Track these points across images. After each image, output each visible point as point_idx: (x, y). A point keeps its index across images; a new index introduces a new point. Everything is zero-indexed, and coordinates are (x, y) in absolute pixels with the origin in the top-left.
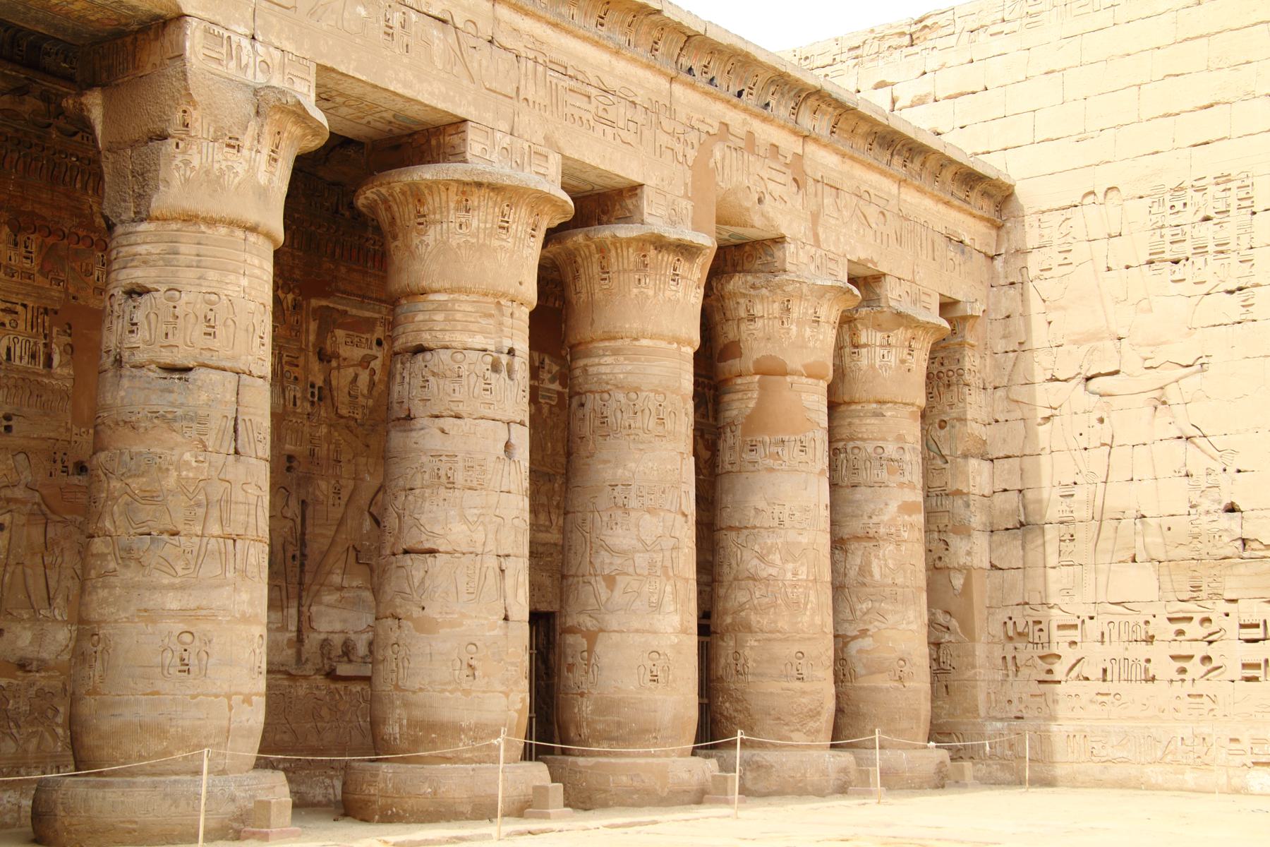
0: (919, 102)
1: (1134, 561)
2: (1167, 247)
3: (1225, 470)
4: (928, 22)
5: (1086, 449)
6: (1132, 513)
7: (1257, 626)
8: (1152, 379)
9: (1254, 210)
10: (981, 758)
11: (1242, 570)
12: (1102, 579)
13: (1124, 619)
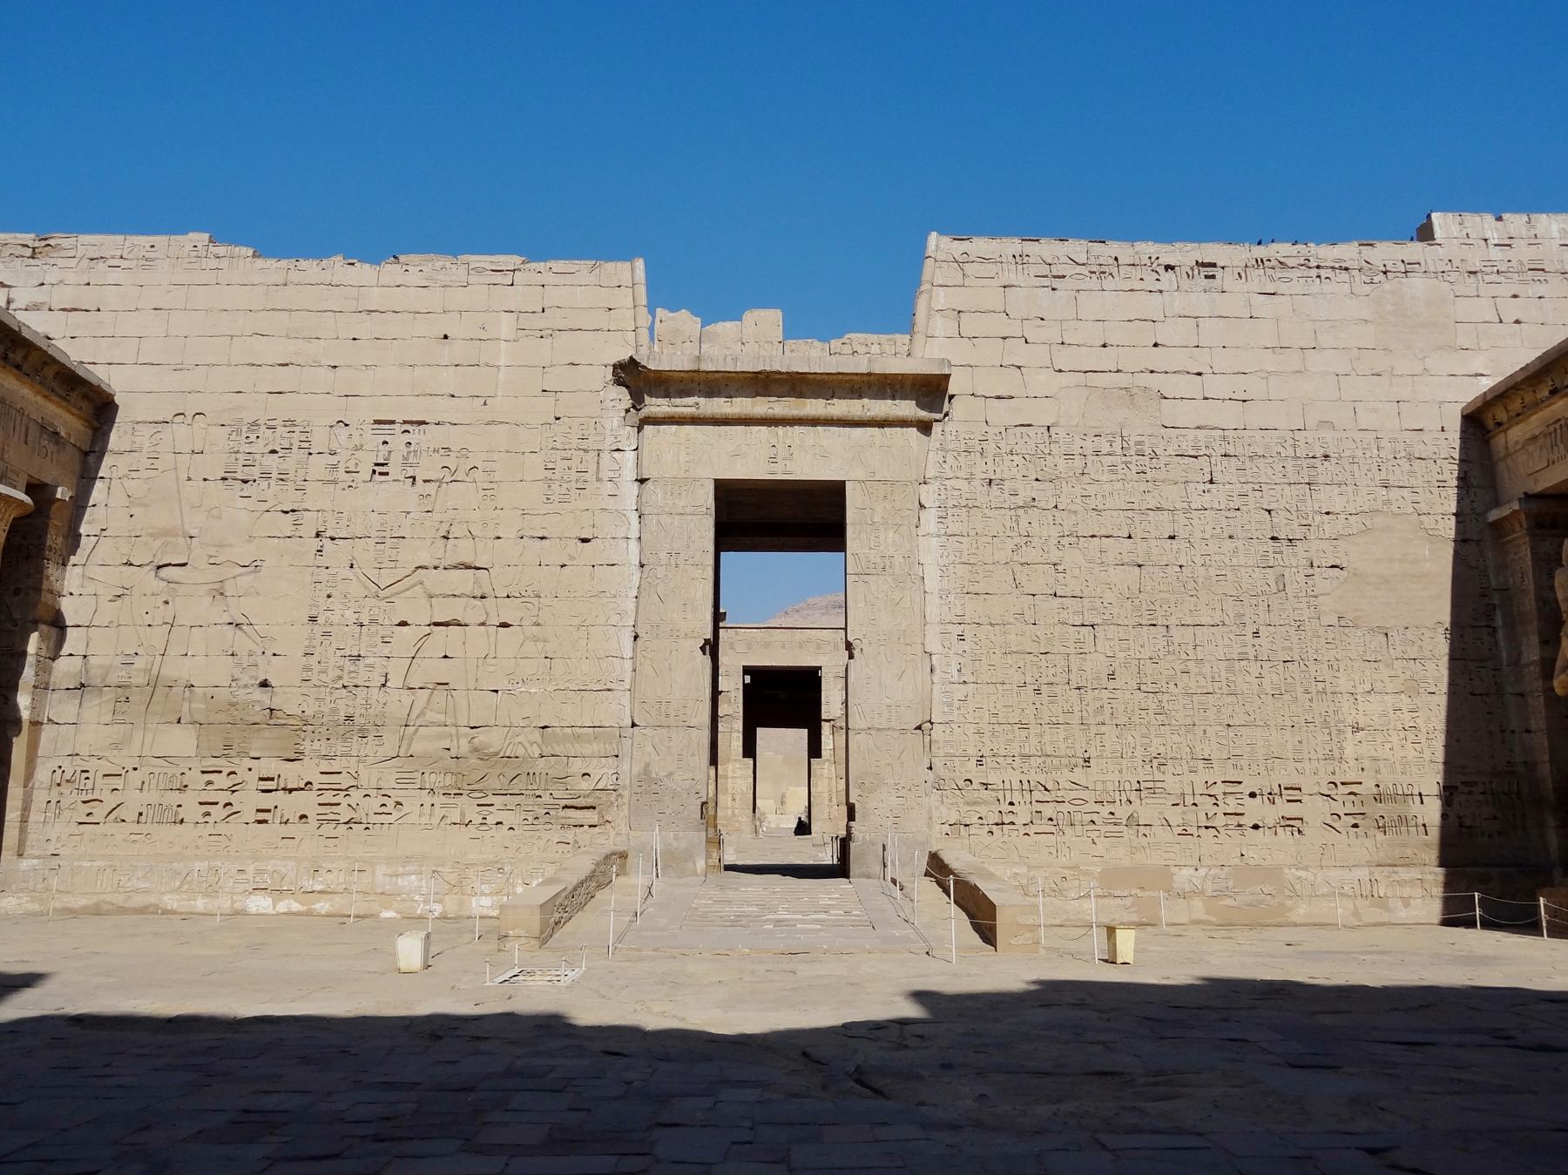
0: (35, 307)
1: (179, 722)
2: (240, 468)
3: (264, 653)
4: (50, 242)
6: (184, 682)
7: (272, 779)
8: (214, 574)
9: (311, 451)
11: (267, 734)
12: (149, 736)
13: (166, 770)
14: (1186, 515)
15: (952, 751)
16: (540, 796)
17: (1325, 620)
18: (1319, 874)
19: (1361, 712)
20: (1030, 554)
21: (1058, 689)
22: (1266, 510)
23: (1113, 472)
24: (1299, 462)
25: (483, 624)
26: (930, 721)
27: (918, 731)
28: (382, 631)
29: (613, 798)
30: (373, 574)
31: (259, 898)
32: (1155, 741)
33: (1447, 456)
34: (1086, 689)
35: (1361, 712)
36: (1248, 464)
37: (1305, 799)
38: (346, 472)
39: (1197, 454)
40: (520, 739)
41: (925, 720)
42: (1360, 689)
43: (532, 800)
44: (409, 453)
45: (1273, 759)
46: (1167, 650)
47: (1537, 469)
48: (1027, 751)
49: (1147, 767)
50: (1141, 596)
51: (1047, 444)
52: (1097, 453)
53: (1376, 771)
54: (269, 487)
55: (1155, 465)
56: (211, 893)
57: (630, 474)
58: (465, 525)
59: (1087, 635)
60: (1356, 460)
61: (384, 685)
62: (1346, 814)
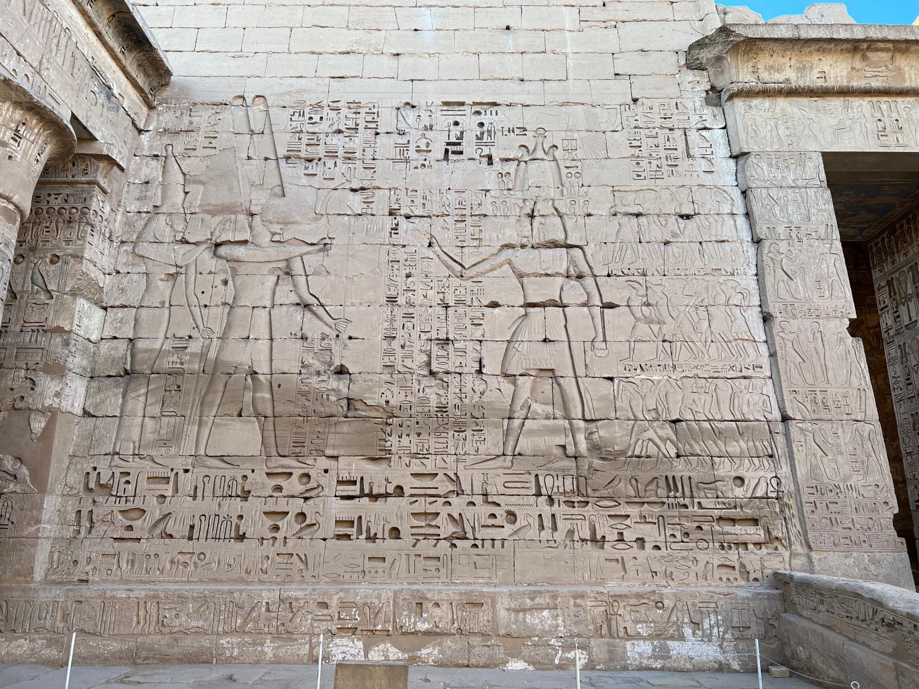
1: (240, 415)
2: (303, 147)
3: (338, 336)
5: (206, 306)
9: (378, 131)
10: (24, 632)
11: (345, 428)
12: (205, 432)
13: (220, 473)
16: (686, 506)
25: (584, 305)
28: (470, 313)
29: (778, 510)
30: (455, 253)
31: (345, 641)
38: (417, 151)
40: (647, 435)
43: (675, 512)
44: (482, 133)
54: (335, 165)
56: (285, 635)
57: (722, 151)
58: (550, 203)
61: (480, 372)
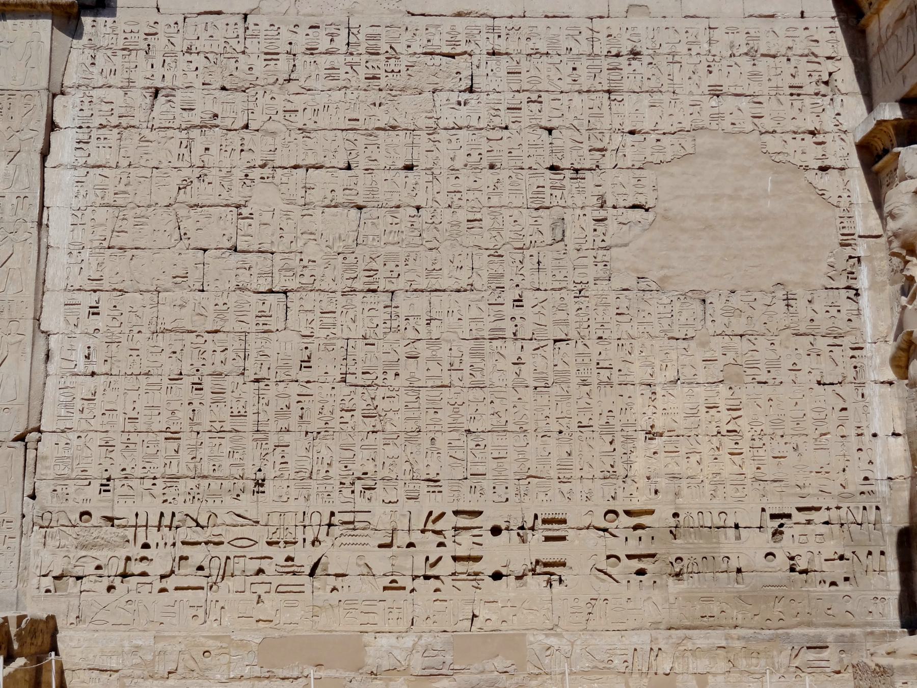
14: (430, 137)
15: (66, 471)
17: (617, 283)
18: (579, 642)
19: (659, 411)
20: (201, 192)
21: (228, 383)
22: (546, 129)
23: (330, 77)
24: (597, 62)
26: (38, 430)
27: (19, 444)
32: (360, 455)
33: (806, 52)
34: (267, 382)
35: (659, 411)
36: (525, 65)
37: (571, 534)
39: (453, 52)
41: (30, 428)
42: (660, 378)
45: (529, 480)
46: (388, 325)
47: (906, 60)
48: (173, 470)
49: (347, 492)
50: (359, 250)
51: (241, 39)
52: (311, 51)
53: (676, 494)
55: (392, 67)
59: (274, 304)
60: (677, 58)
62: (629, 557)
